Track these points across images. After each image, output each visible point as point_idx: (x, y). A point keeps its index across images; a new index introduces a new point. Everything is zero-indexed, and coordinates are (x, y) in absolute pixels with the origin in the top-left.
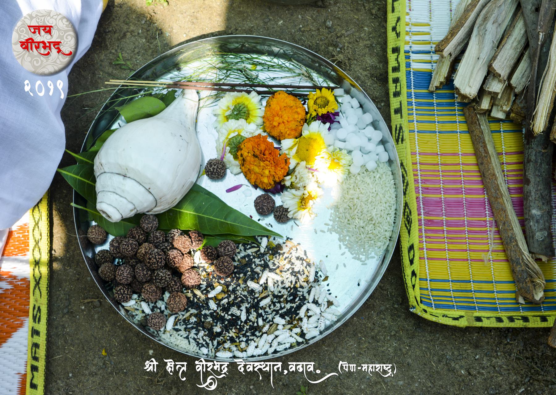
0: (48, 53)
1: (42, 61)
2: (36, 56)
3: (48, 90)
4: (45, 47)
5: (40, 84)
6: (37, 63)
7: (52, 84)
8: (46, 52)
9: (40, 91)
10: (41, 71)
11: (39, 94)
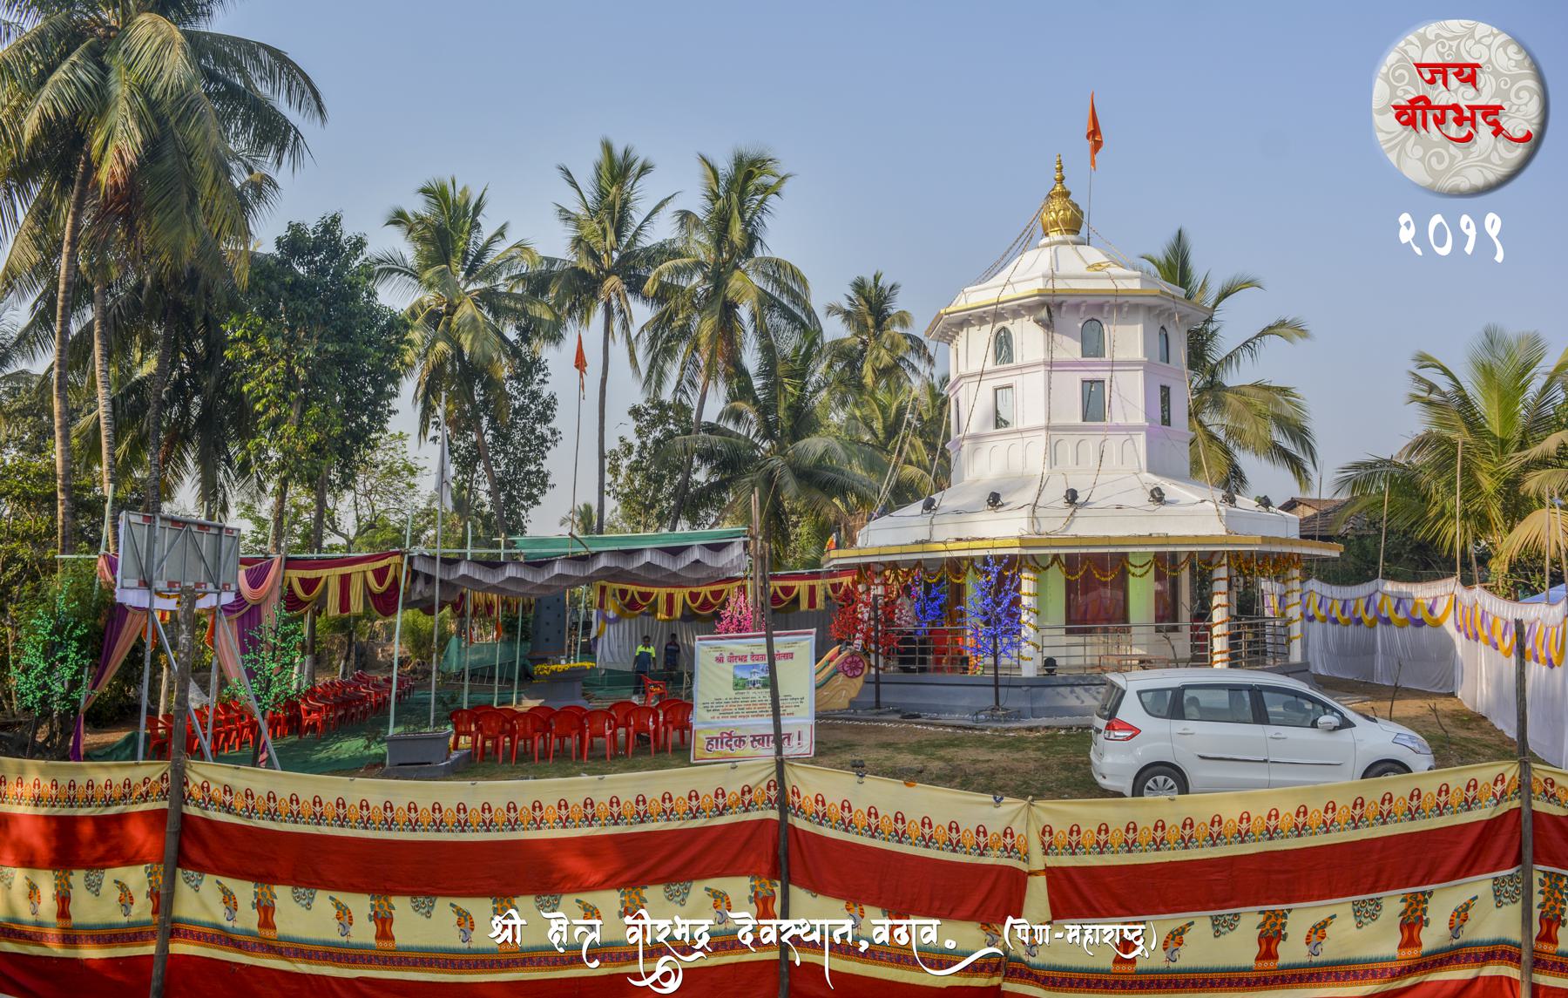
0: (1469, 137)
1: (1452, 158)
3: (1461, 239)
4: (1459, 121)
5: (1440, 225)
7: (1472, 225)
8: (1464, 134)
9: (1441, 242)
10: (1448, 183)
11: (1439, 250)
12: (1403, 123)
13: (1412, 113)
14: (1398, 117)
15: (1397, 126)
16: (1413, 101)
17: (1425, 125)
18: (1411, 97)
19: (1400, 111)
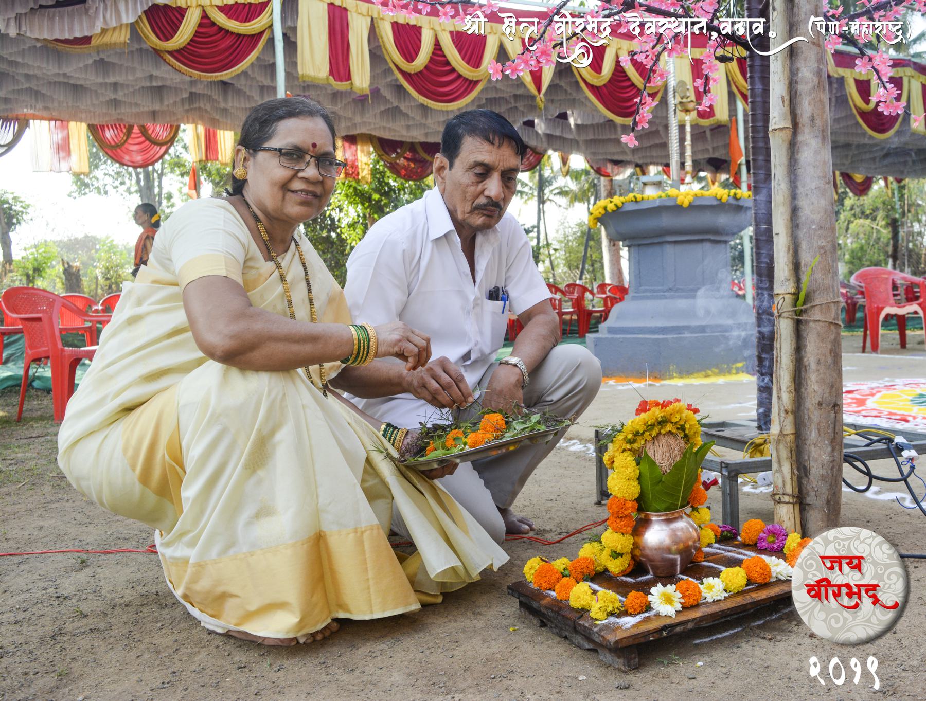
0: (856, 606)
1: (845, 619)
4: (850, 595)
6: (837, 622)
8: (853, 604)
10: (842, 637)
12: (812, 596)
13: (818, 589)
14: (809, 592)
15: (810, 599)
16: (819, 582)
17: (827, 598)
19: (810, 588)
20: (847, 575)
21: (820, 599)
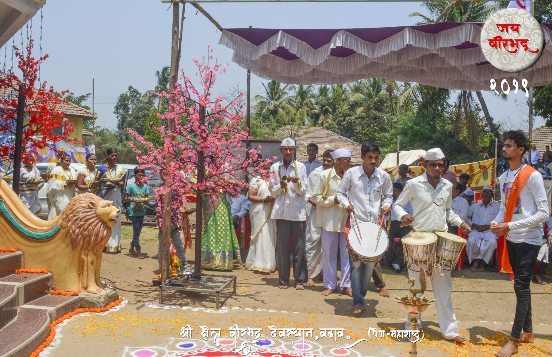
0: (516, 51)
1: (510, 58)
2: (504, 54)
4: (512, 45)
7: (517, 83)
8: (514, 50)
10: (507, 68)
12: (492, 46)
13: (495, 42)
14: (490, 43)
15: (490, 47)
17: (500, 47)
18: (494, 36)
19: (491, 41)
20: (511, 34)
21: (496, 47)
